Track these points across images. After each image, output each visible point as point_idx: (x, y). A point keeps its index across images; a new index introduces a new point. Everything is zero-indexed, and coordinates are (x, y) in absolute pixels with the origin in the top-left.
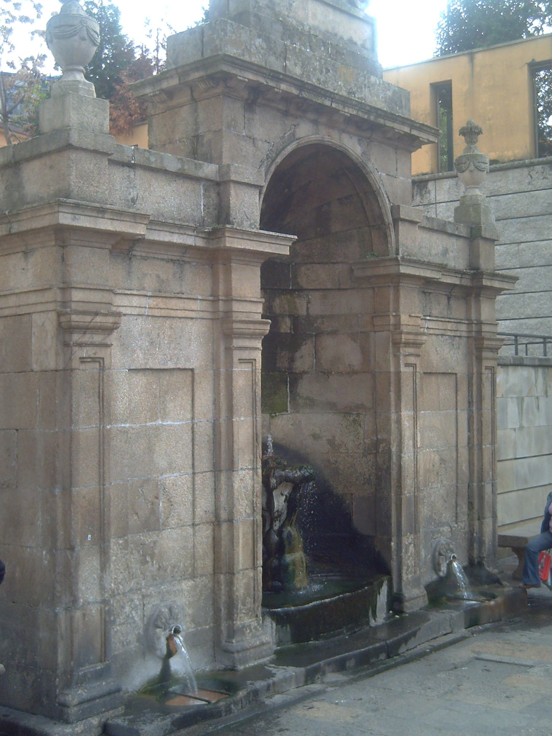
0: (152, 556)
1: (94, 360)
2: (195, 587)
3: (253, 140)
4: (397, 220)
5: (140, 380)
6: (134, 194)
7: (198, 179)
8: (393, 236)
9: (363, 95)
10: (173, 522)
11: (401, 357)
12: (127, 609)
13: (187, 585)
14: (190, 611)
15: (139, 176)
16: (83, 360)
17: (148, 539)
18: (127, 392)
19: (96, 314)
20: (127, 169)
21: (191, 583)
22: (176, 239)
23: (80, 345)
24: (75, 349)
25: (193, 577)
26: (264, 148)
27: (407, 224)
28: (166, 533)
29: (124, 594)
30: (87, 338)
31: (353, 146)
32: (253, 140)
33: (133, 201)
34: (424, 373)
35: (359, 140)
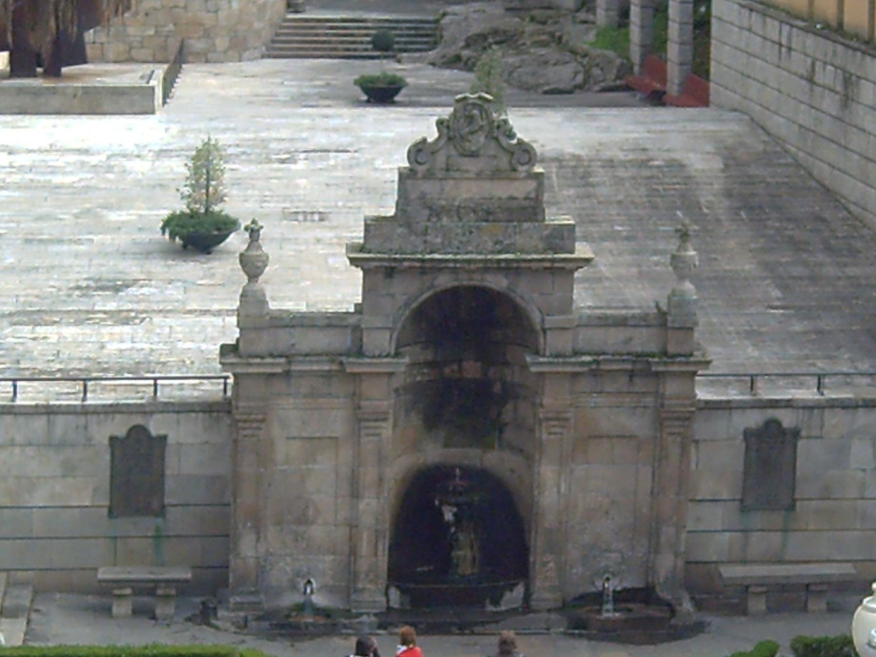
0: (303, 538)
1: (253, 436)
2: (334, 560)
3: (392, 296)
4: (544, 331)
5: (297, 444)
6: (292, 342)
7: (346, 327)
9: (513, 240)
10: (320, 521)
12: (281, 564)
13: (329, 558)
14: (331, 573)
15: (297, 332)
16: (245, 436)
17: (301, 529)
18: (286, 451)
19: (250, 414)
20: (288, 329)
21: (332, 557)
22: (315, 368)
23: (244, 429)
24: (241, 431)
25: (333, 553)
26: (401, 299)
28: (314, 527)
29: (280, 556)
30: (247, 425)
31: (497, 282)
32: (392, 296)
33: (293, 345)
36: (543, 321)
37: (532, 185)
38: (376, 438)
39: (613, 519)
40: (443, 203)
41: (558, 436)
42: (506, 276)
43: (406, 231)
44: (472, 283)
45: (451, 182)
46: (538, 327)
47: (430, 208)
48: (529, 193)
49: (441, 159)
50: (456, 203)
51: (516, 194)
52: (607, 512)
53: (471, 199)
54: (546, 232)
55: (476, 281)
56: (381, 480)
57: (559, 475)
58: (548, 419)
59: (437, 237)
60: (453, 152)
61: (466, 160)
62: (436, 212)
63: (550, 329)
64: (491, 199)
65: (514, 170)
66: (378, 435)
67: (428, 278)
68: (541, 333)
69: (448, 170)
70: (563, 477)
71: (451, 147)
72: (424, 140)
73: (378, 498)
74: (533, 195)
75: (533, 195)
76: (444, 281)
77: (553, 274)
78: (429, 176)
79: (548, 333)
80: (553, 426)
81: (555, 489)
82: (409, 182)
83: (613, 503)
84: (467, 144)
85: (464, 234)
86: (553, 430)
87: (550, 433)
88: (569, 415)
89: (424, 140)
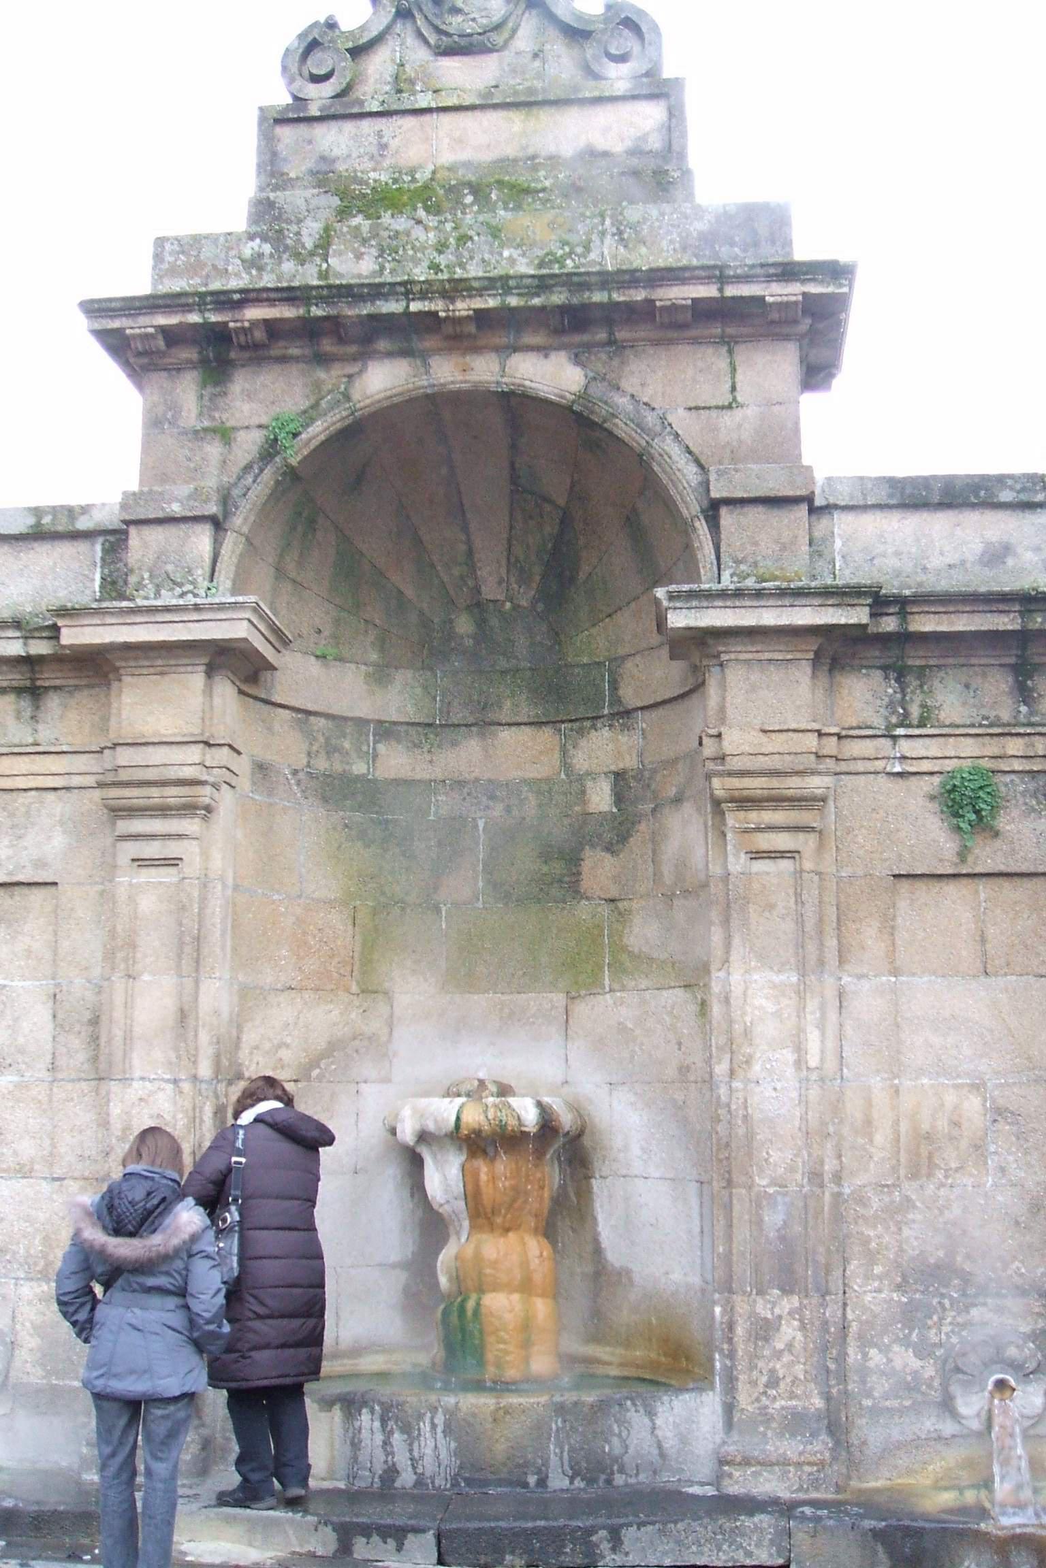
8: (708, 548)
11: (729, 836)
27: (755, 514)
31: (552, 375)
34: (896, 876)
35: (576, 355)
36: (706, 485)
37: (650, 115)
38: (167, 876)
39: (1003, 1170)
40: (384, 177)
41: (785, 865)
42: (577, 360)
43: (267, 248)
44: (473, 377)
45: (409, 122)
46: (691, 506)
47: (343, 194)
48: (644, 138)
49: (379, 66)
50: (423, 176)
51: (601, 144)
52: (978, 1148)
53: (467, 164)
54: (700, 226)
55: (484, 370)
56: (184, 1016)
57: (801, 993)
58: (745, 802)
59: (359, 256)
60: (419, 55)
61: (448, 63)
62: (359, 200)
63: (729, 502)
64: (533, 158)
65: (597, 77)
66: (172, 862)
67: (330, 377)
68: (702, 527)
69: (400, 91)
70: (812, 1005)
71: (411, 40)
72: (331, 25)
73: (175, 1082)
74: (655, 143)
75: (655, 143)
76: (382, 379)
77: (729, 343)
78: (345, 109)
79: (724, 511)
80: (771, 828)
81: (789, 1056)
82: (286, 134)
83: (999, 1113)
84: (457, 20)
85: (441, 248)
86: (766, 841)
87: (757, 855)
88: (816, 784)
89: (331, 25)
